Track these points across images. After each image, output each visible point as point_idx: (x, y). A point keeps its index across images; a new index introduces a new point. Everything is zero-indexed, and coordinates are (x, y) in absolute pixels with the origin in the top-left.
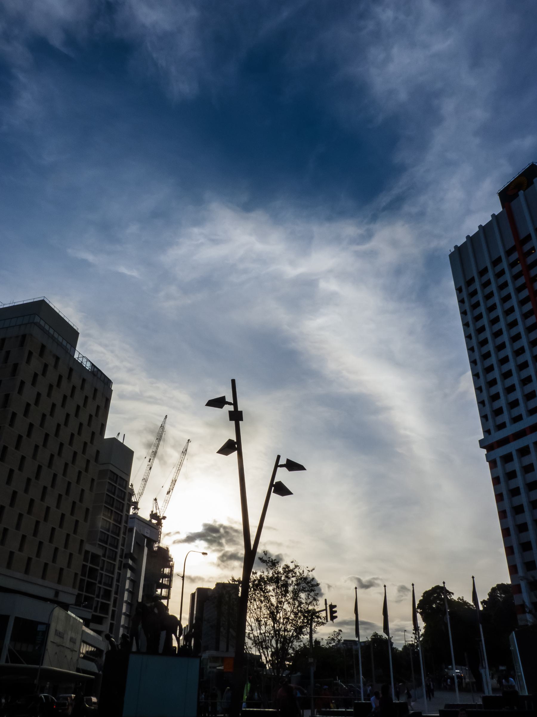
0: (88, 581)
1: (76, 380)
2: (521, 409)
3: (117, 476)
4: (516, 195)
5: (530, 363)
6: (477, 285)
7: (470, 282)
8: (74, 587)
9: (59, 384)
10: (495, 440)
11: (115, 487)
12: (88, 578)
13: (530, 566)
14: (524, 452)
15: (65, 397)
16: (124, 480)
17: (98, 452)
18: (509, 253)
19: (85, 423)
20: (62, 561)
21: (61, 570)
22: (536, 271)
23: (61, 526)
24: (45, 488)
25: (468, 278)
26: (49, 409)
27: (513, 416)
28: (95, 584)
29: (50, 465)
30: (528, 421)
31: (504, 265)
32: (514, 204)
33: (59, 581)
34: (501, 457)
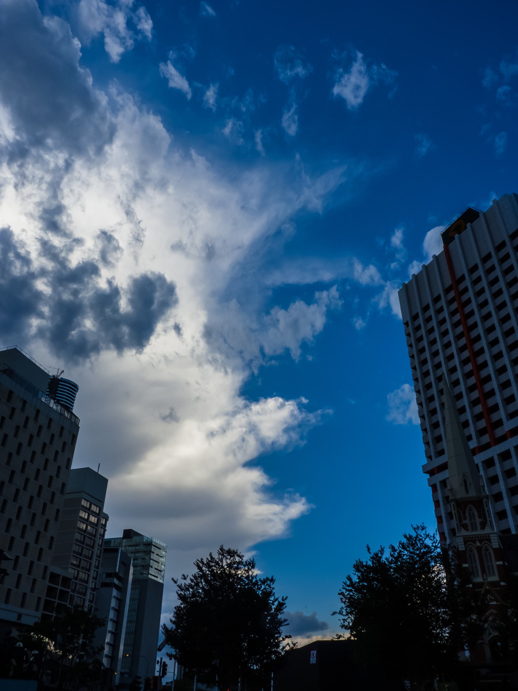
1: (43, 420)
4: (453, 238)
6: (421, 321)
7: (415, 317)
9: (25, 426)
10: (435, 466)
12: (58, 600)
15: (31, 437)
17: (64, 485)
18: (447, 291)
19: (51, 459)
20: (25, 586)
21: (25, 594)
23: (25, 554)
24: (10, 520)
29: (15, 499)
31: (443, 302)
33: (22, 605)
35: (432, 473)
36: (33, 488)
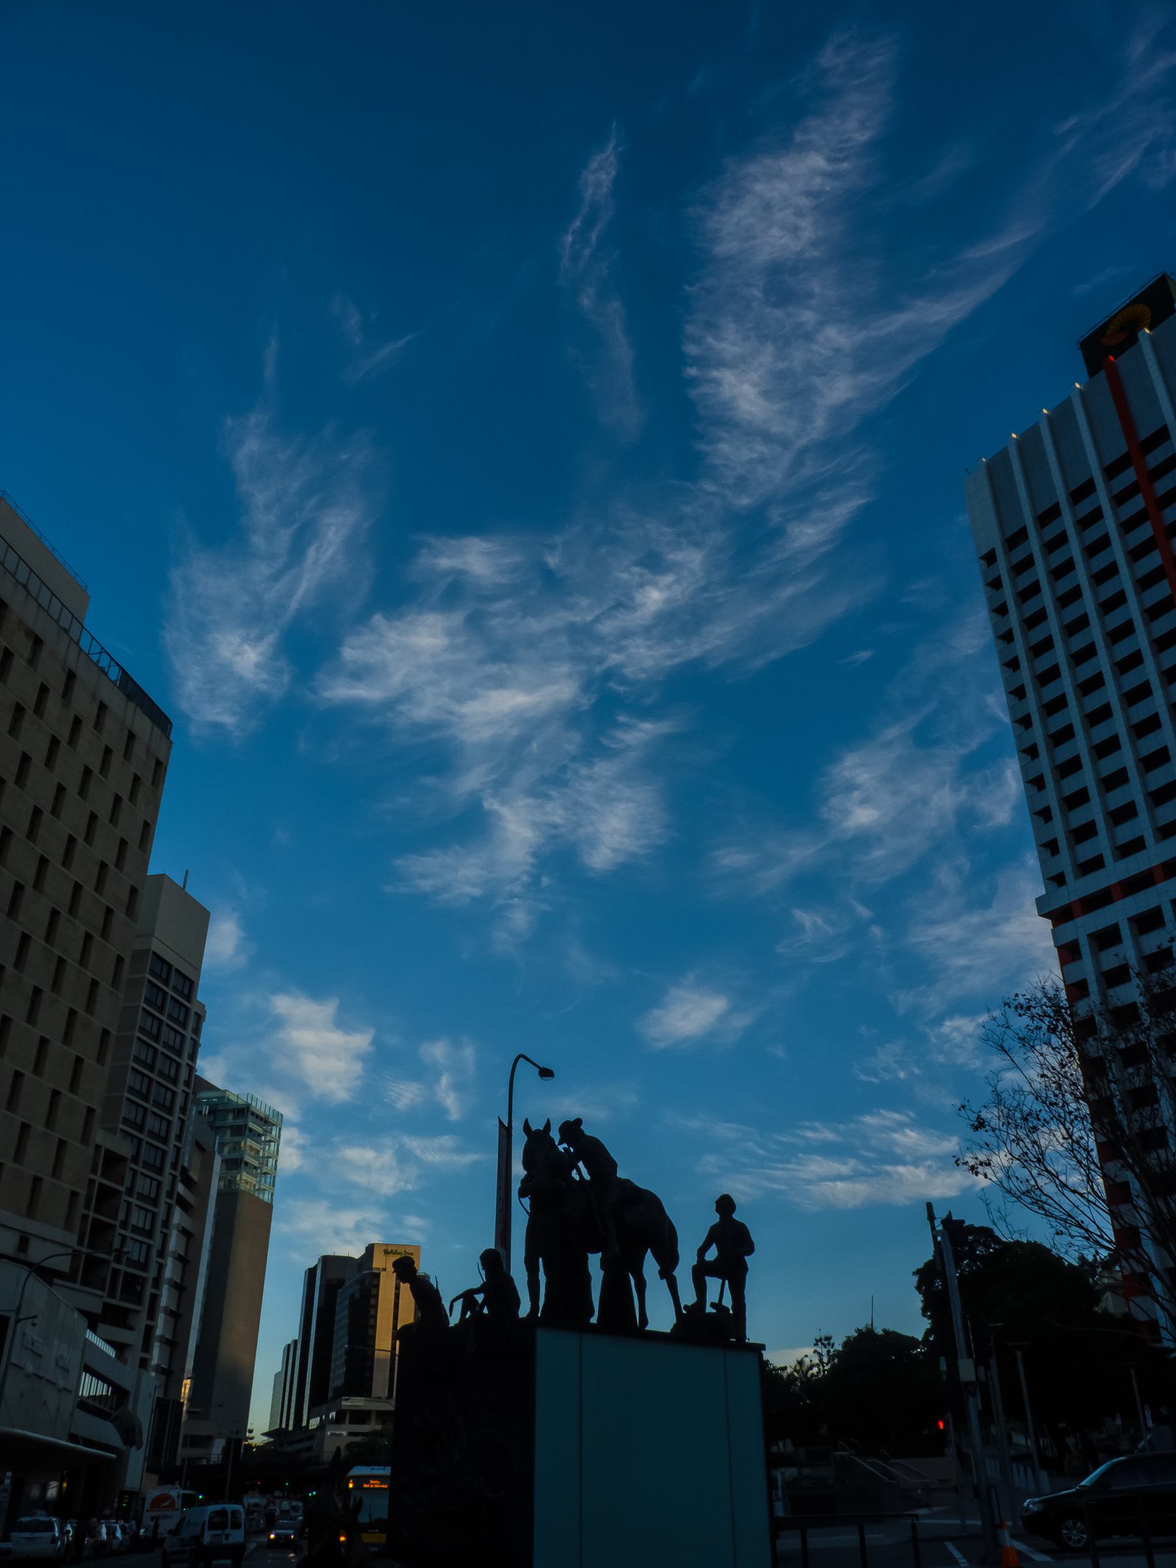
0: (94, 1220)
2: (1142, 825)
3: (170, 966)
5: (1165, 718)
8: (68, 1226)
10: (1074, 898)
11: (165, 993)
12: (96, 1211)
13: (1162, 1183)
14: (1149, 921)
15: (55, 742)
16: (185, 978)
17: (134, 890)
18: (1111, 471)
22: (1175, 513)
23: (38, 1068)
25: (1012, 530)
26: (14, 769)
27: (1120, 842)
28: (113, 1227)
30: (1156, 854)
32: (1124, 363)
34: (1090, 936)
35: (1059, 916)
36: (58, 885)
